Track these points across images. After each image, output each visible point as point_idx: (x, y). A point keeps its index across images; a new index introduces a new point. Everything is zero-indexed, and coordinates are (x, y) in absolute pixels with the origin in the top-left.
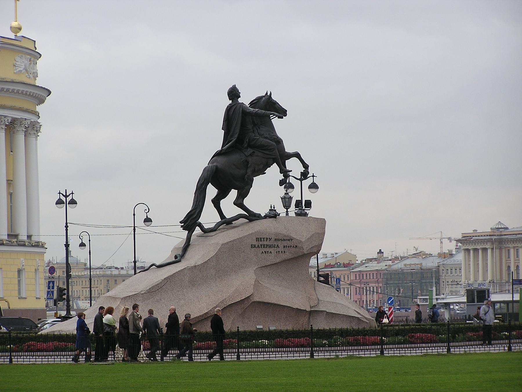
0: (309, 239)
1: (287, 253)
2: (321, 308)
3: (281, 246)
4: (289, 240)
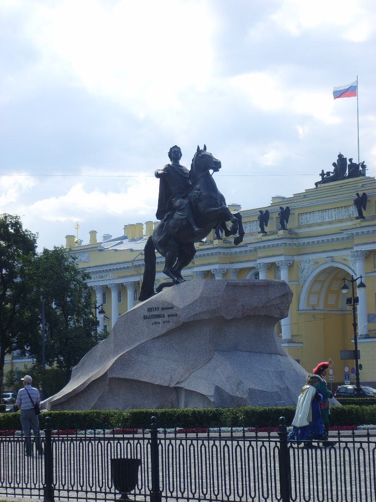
0: (190, 305)
1: (171, 323)
2: (182, 385)
3: (166, 316)
4: (171, 308)
